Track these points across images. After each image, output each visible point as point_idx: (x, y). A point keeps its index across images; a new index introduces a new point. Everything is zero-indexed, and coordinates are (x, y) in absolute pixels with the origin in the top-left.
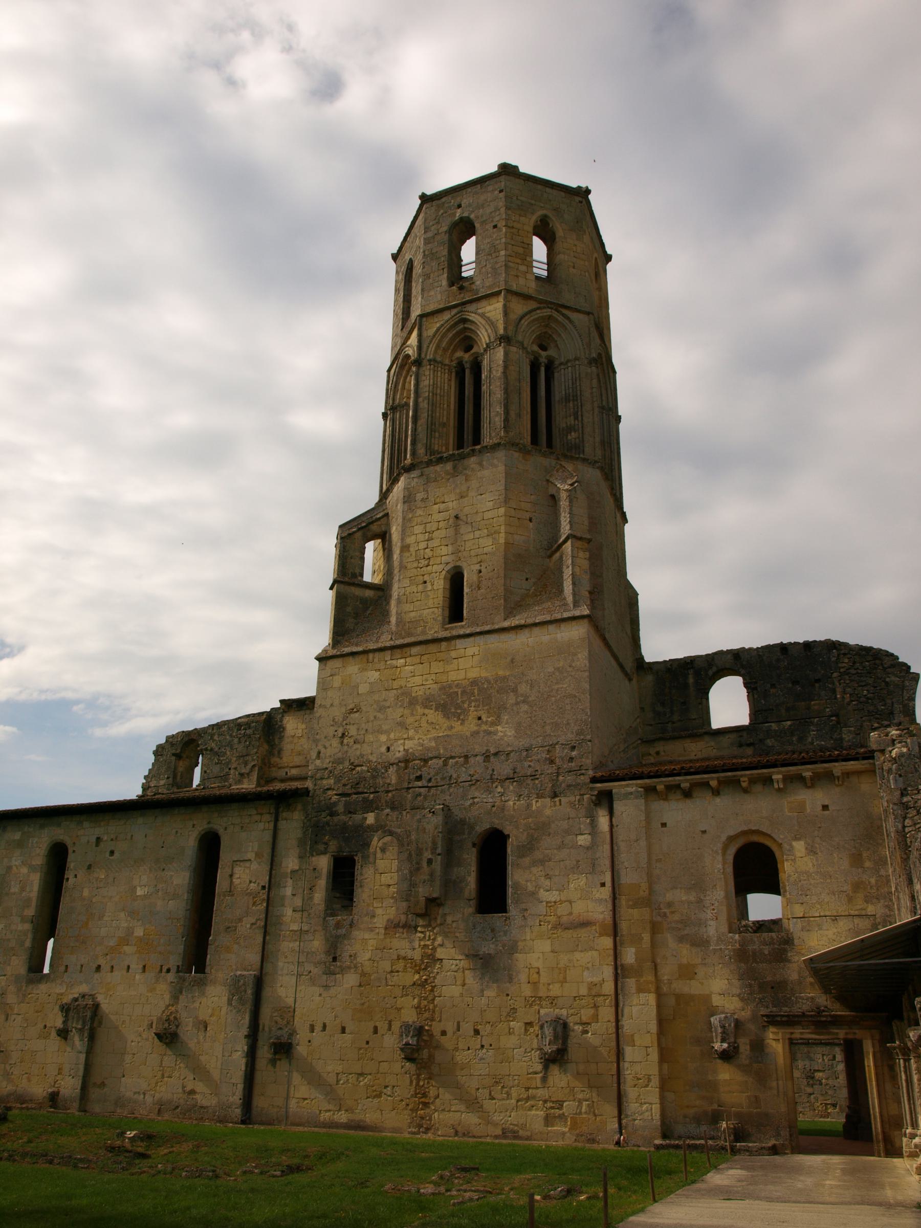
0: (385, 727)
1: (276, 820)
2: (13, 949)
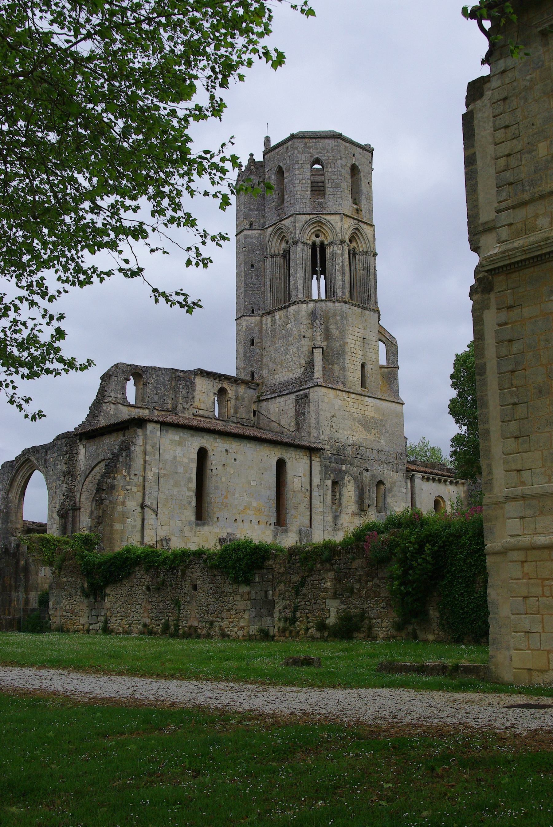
0: (346, 428)
1: (311, 460)
2: (184, 505)
